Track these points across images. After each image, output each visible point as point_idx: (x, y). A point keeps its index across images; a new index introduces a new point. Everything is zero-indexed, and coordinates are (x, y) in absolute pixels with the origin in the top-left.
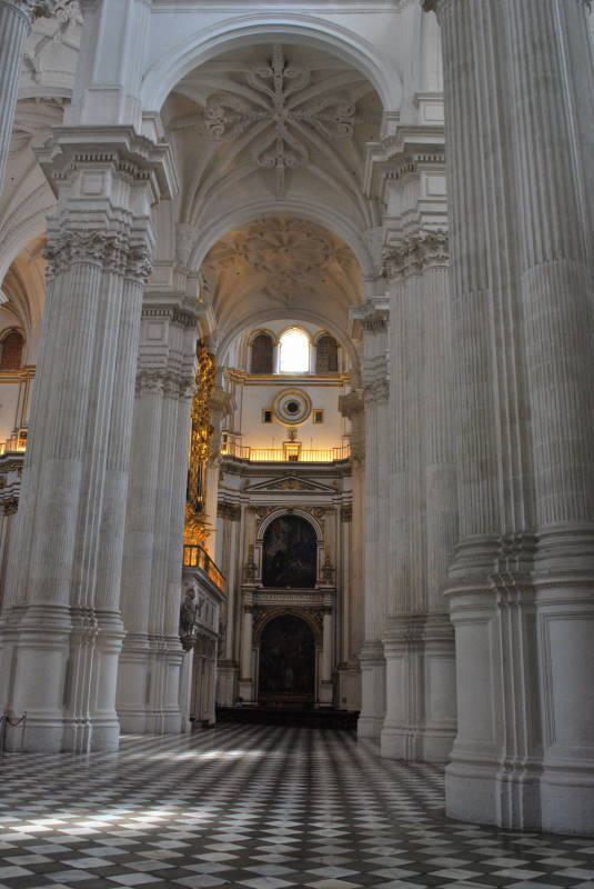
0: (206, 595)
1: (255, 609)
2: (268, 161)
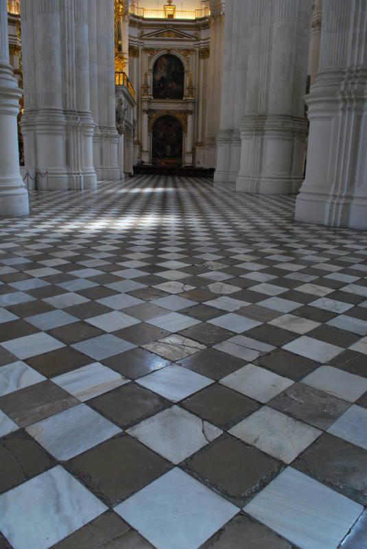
0: (127, 103)
1: (149, 111)
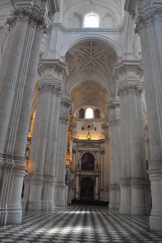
0: (71, 172)
1: (79, 175)
2: (87, 68)
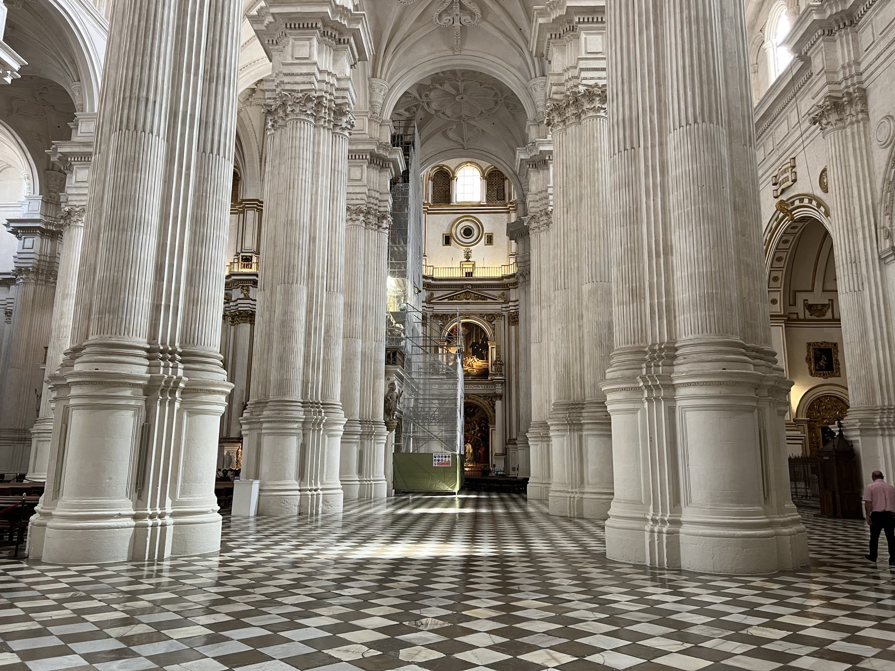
2: (446, 19)
